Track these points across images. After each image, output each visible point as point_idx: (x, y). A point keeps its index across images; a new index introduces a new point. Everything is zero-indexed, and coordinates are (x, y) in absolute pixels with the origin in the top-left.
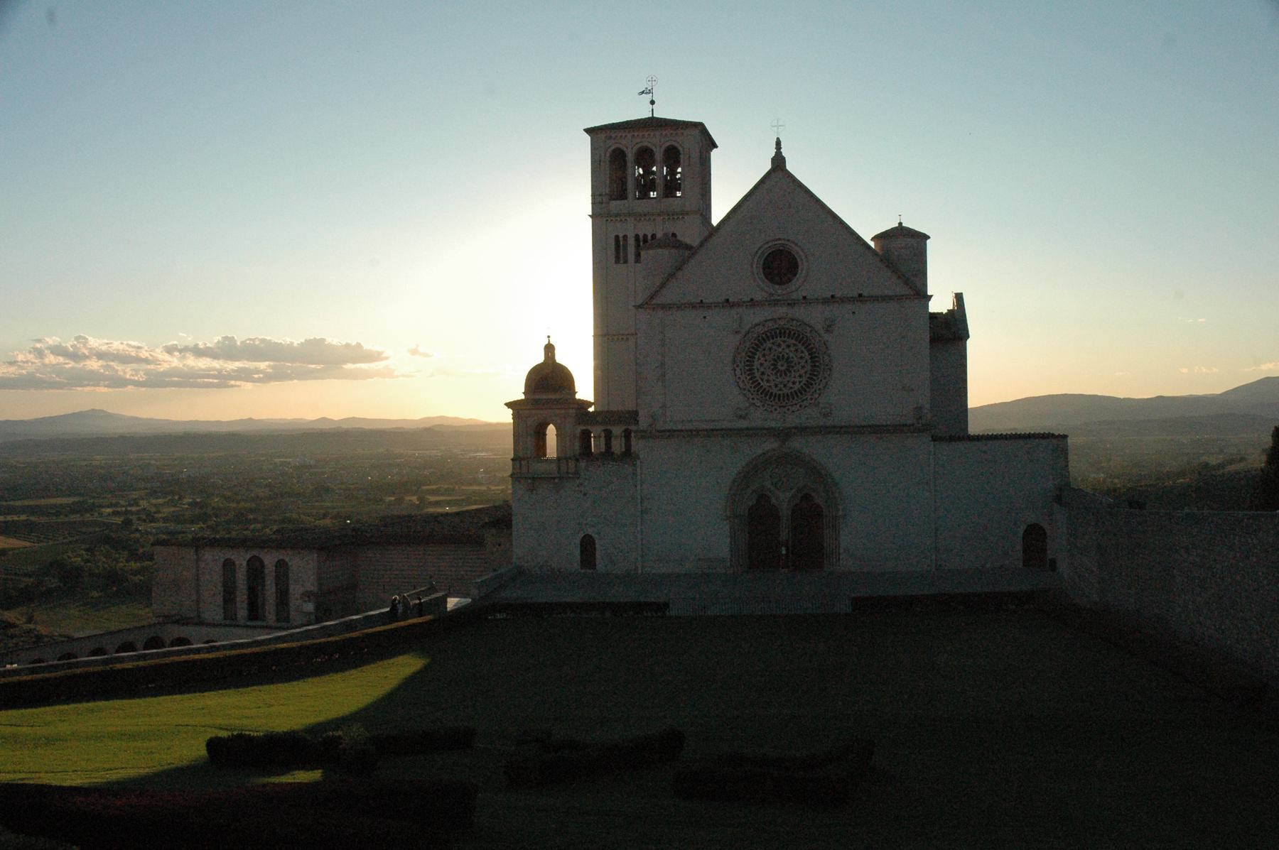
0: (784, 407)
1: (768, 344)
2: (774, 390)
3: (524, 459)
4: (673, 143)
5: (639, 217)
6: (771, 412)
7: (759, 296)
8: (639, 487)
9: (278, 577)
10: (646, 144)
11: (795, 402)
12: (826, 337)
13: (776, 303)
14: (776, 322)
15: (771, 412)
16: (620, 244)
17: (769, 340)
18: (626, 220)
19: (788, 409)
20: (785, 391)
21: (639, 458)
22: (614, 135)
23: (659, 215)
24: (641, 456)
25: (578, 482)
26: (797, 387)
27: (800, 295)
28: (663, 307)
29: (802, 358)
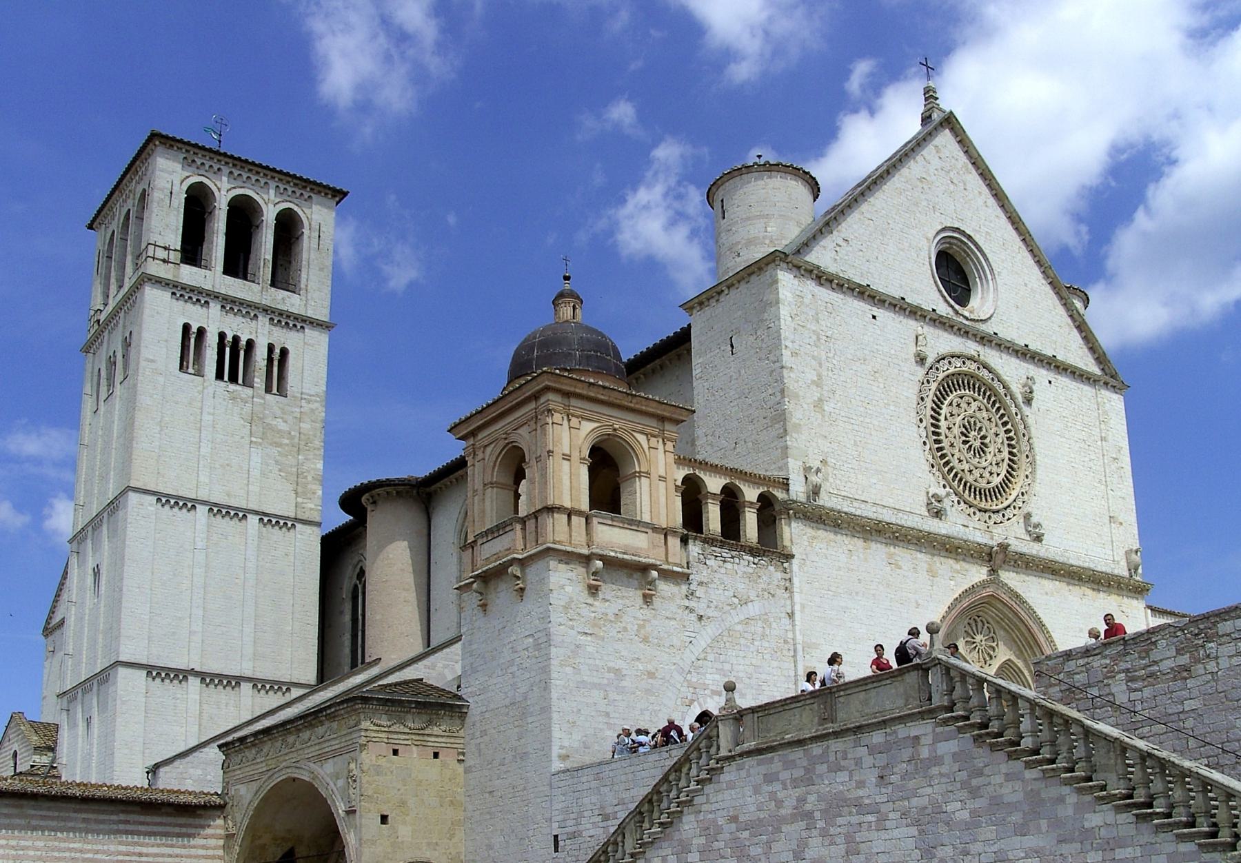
0: (985, 511)
2: (970, 478)
3: (579, 513)
5: (230, 304)
6: (969, 515)
8: (797, 616)
11: (994, 507)
12: (1026, 410)
13: (964, 333)
14: (964, 363)
15: (969, 515)
16: (192, 339)
17: (956, 391)
18: (206, 302)
19: (990, 517)
20: (983, 484)
21: (793, 556)
25: (684, 587)
26: (996, 481)
28: (822, 278)
29: (997, 435)
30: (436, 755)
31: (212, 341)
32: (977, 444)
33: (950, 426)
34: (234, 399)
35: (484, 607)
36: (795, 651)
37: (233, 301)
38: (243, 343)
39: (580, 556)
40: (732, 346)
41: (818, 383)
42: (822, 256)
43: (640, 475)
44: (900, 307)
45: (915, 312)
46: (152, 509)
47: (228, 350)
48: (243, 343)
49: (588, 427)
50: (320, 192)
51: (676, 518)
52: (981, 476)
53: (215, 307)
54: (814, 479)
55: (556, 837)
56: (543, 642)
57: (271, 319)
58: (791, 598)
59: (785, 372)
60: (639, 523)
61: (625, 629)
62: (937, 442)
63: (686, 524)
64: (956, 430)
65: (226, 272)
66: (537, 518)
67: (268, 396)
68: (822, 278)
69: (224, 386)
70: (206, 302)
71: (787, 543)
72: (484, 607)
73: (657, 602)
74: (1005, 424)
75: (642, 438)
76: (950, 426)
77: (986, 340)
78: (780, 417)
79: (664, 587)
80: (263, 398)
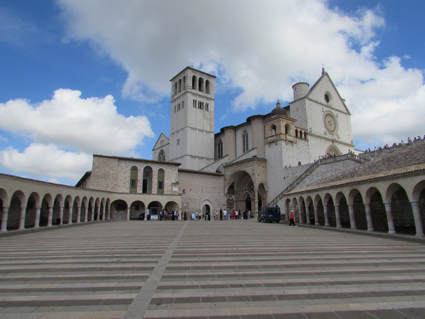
0: (332, 134)
1: (327, 117)
4: (209, 80)
5: (200, 96)
7: (326, 104)
8: (309, 149)
9: (159, 177)
10: (202, 77)
12: (337, 118)
16: (195, 102)
18: (197, 96)
20: (331, 130)
22: (194, 72)
23: (205, 97)
24: (309, 140)
26: (333, 129)
27: (332, 106)
28: (311, 100)
30: (263, 167)
31: (198, 102)
32: (330, 124)
33: (327, 121)
34: (201, 112)
35: (269, 147)
36: (309, 154)
37: (200, 96)
38: (202, 103)
39: (285, 140)
40: (297, 110)
41: (311, 116)
42: (310, 97)
43: (290, 129)
44: (320, 104)
45: (322, 104)
46: (190, 130)
47: (200, 104)
48: (202, 103)
49: (285, 122)
50: (212, 77)
51: (295, 135)
52: (331, 129)
53: (198, 96)
54: (311, 129)
55: (284, 177)
56: (281, 152)
57: (206, 99)
58: (309, 146)
59: (307, 114)
60: (291, 136)
61: (290, 150)
62: (325, 124)
63: (296, 136)
64: (328, 122)
65: (200, 90)
66: (279, 135)
67: (206, 112)
68: (311, 100)
69: (199, 110)
70: (197, 96)
71: (308, 138)
72: (269, 147)
73: (293, 147)
74: (334, 121)
75: (290, 124)
76: (327, 121)
77: (332, 108)
78: (306, 121)
79: (294, 145)
80: (205, 112)
